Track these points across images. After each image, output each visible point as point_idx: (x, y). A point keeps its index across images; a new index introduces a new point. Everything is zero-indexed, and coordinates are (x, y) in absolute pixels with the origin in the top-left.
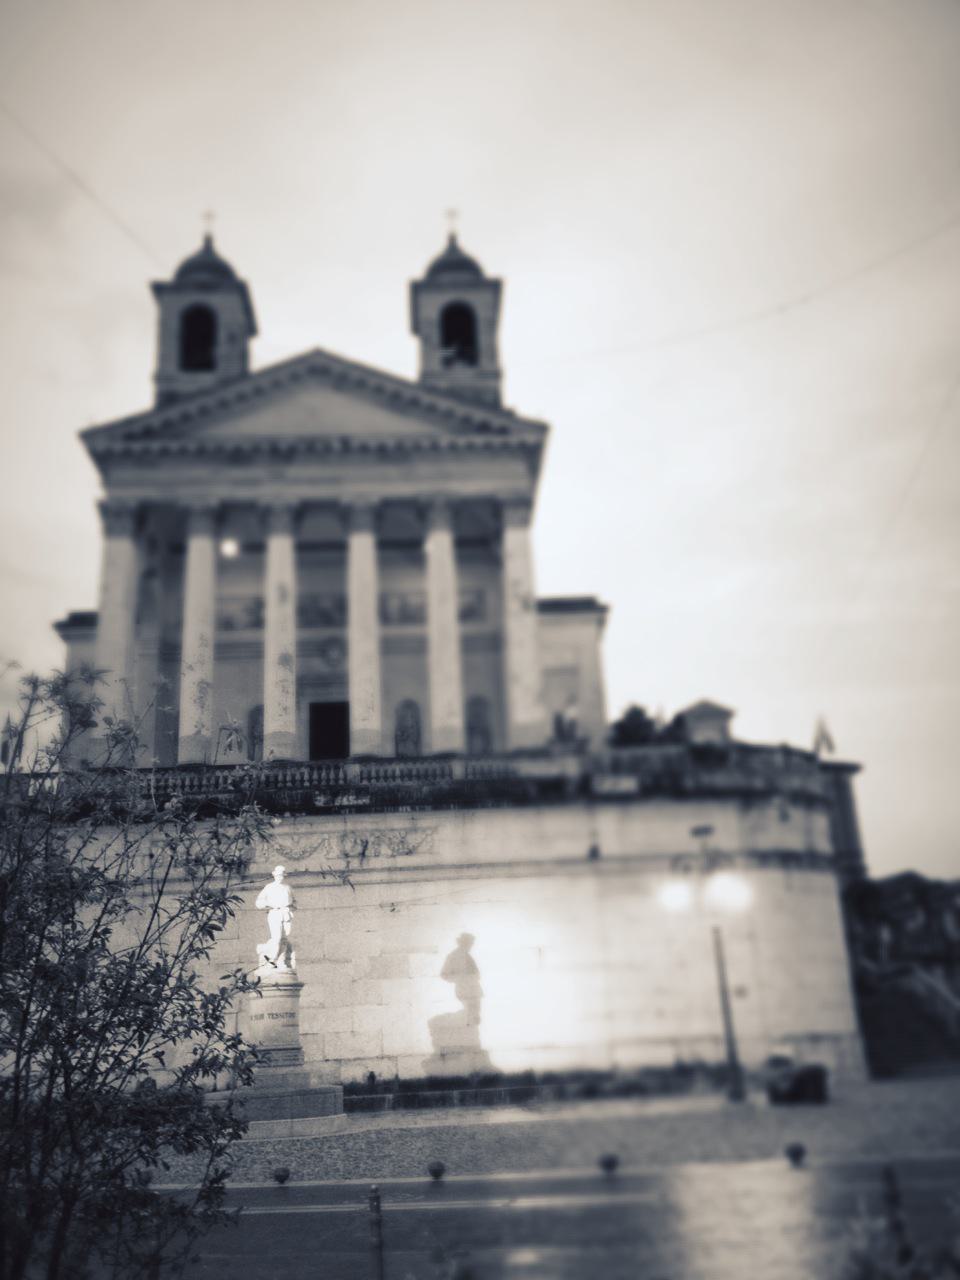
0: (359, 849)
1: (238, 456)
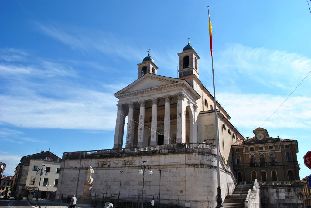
0: (125, 163)
1: (136, 94)
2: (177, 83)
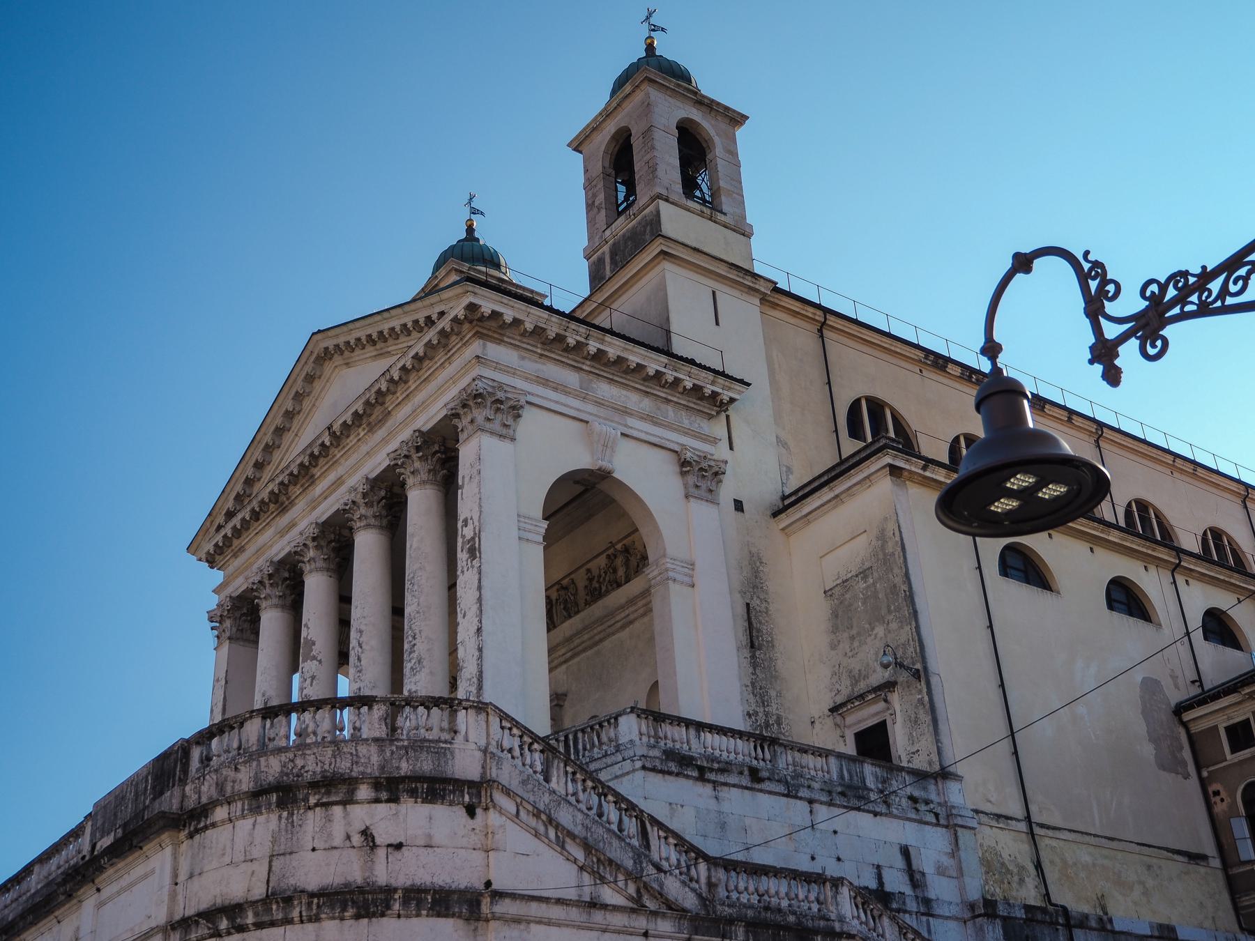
2: (440, 325)
